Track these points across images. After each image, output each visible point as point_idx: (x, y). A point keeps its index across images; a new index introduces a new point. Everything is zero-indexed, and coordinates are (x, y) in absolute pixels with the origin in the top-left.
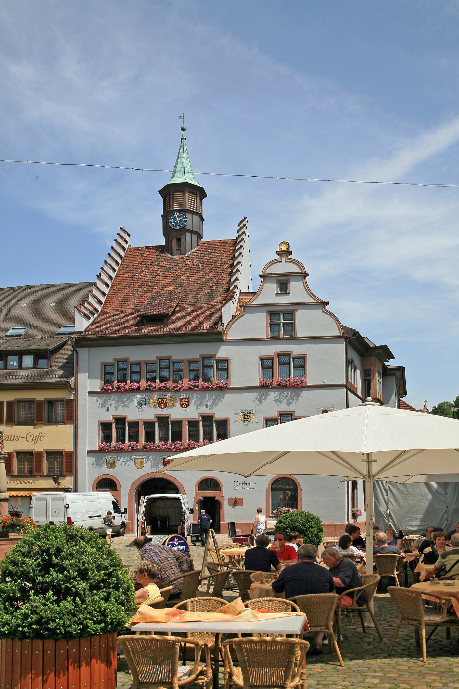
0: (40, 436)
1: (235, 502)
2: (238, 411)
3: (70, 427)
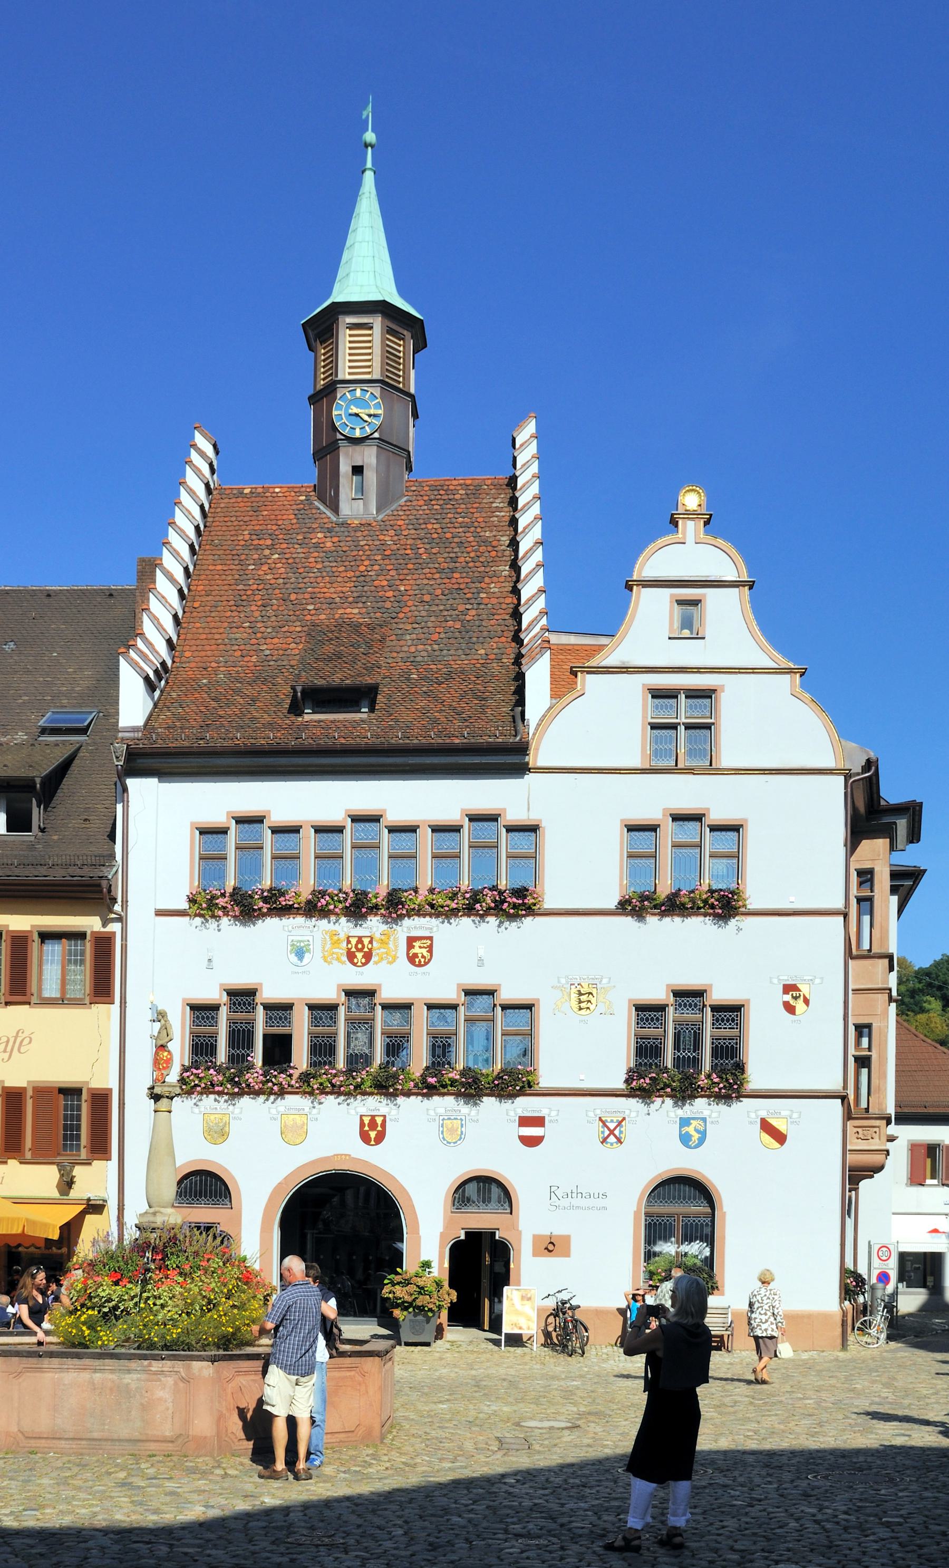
0: (19, 1040)
2: (563, 981)
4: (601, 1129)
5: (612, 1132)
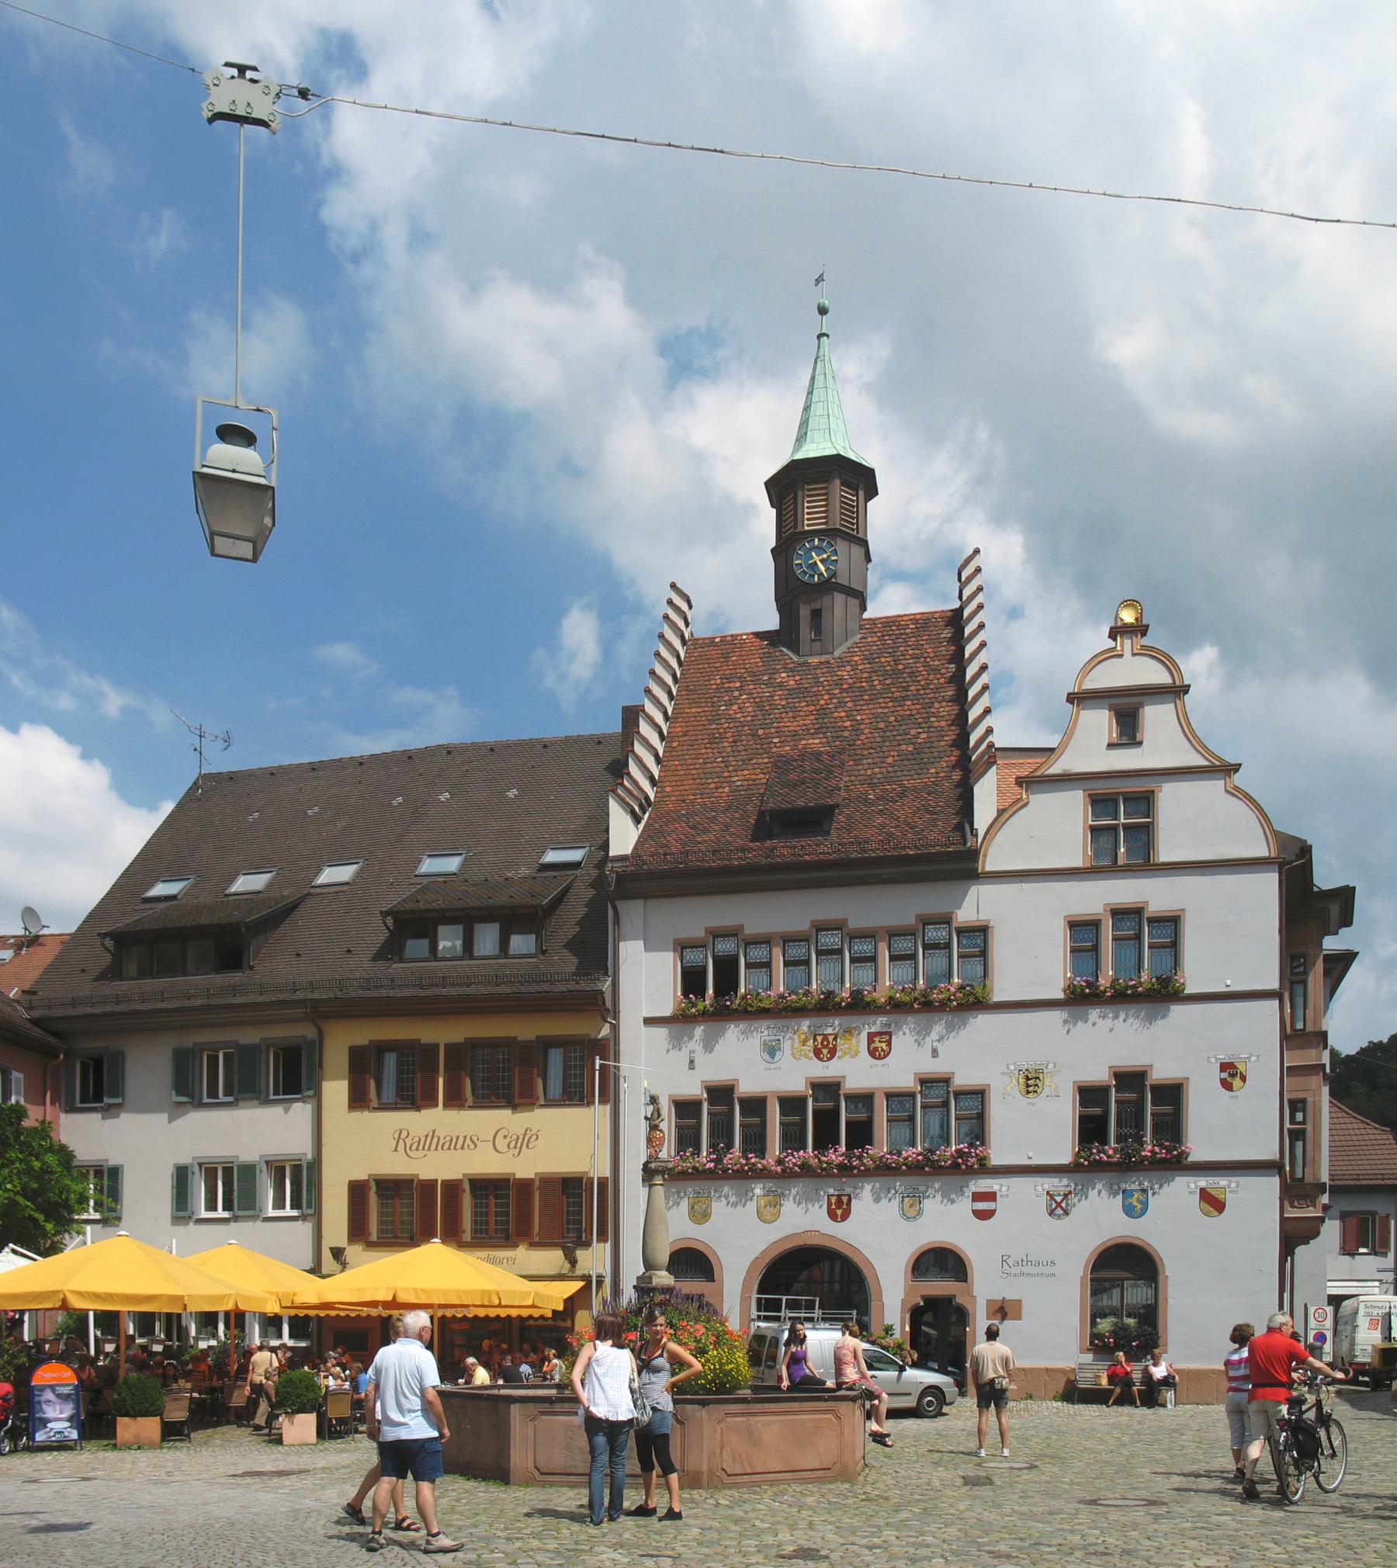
1: (1003, 1310)
3: (600, 1113)
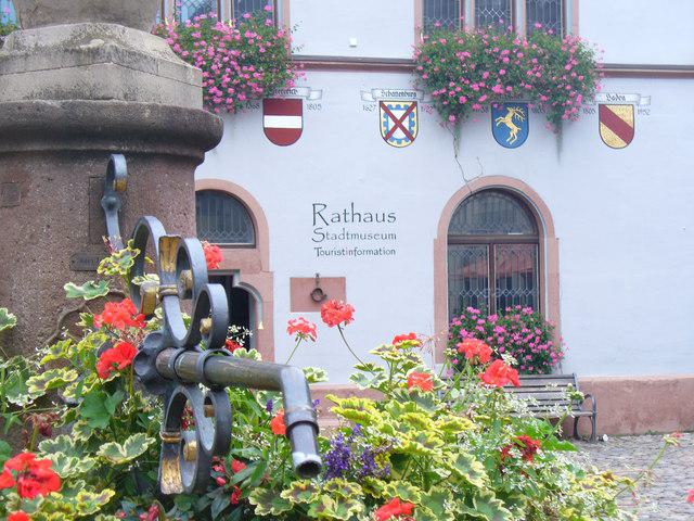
4: (383, 119)
5: (398, 123)
